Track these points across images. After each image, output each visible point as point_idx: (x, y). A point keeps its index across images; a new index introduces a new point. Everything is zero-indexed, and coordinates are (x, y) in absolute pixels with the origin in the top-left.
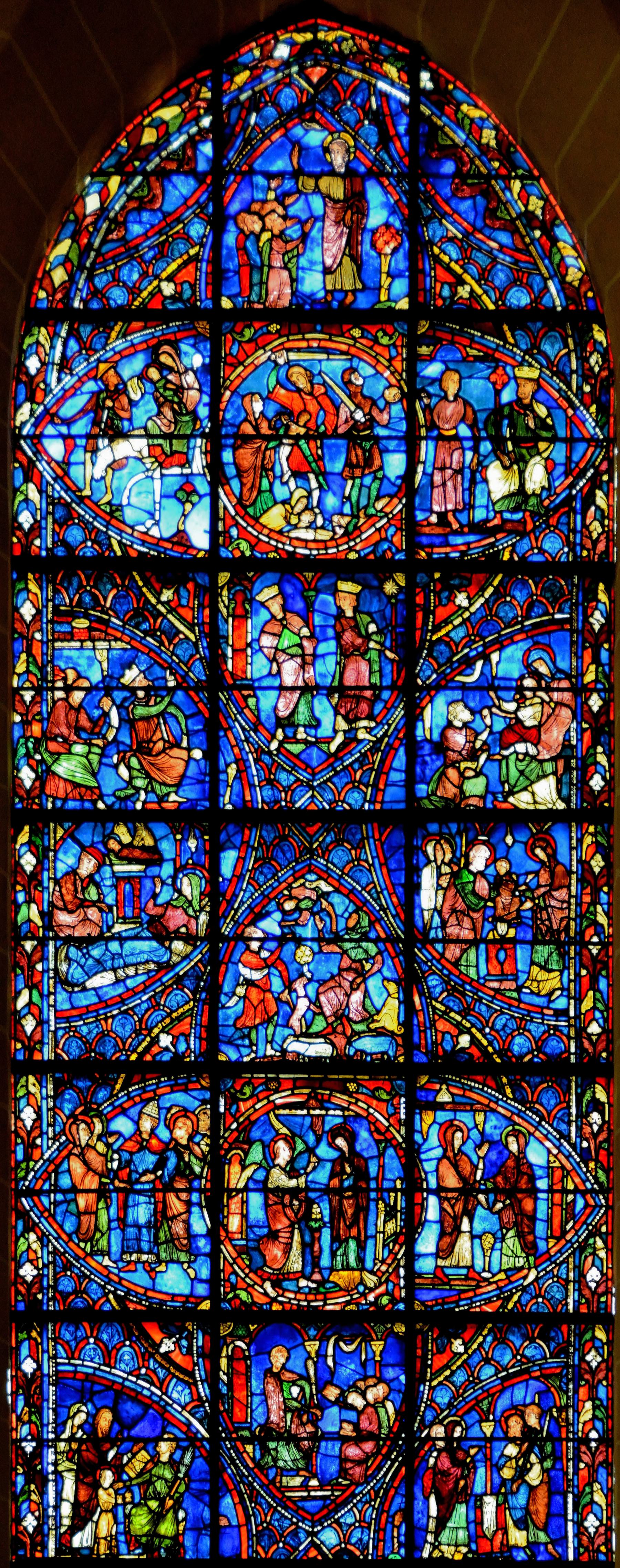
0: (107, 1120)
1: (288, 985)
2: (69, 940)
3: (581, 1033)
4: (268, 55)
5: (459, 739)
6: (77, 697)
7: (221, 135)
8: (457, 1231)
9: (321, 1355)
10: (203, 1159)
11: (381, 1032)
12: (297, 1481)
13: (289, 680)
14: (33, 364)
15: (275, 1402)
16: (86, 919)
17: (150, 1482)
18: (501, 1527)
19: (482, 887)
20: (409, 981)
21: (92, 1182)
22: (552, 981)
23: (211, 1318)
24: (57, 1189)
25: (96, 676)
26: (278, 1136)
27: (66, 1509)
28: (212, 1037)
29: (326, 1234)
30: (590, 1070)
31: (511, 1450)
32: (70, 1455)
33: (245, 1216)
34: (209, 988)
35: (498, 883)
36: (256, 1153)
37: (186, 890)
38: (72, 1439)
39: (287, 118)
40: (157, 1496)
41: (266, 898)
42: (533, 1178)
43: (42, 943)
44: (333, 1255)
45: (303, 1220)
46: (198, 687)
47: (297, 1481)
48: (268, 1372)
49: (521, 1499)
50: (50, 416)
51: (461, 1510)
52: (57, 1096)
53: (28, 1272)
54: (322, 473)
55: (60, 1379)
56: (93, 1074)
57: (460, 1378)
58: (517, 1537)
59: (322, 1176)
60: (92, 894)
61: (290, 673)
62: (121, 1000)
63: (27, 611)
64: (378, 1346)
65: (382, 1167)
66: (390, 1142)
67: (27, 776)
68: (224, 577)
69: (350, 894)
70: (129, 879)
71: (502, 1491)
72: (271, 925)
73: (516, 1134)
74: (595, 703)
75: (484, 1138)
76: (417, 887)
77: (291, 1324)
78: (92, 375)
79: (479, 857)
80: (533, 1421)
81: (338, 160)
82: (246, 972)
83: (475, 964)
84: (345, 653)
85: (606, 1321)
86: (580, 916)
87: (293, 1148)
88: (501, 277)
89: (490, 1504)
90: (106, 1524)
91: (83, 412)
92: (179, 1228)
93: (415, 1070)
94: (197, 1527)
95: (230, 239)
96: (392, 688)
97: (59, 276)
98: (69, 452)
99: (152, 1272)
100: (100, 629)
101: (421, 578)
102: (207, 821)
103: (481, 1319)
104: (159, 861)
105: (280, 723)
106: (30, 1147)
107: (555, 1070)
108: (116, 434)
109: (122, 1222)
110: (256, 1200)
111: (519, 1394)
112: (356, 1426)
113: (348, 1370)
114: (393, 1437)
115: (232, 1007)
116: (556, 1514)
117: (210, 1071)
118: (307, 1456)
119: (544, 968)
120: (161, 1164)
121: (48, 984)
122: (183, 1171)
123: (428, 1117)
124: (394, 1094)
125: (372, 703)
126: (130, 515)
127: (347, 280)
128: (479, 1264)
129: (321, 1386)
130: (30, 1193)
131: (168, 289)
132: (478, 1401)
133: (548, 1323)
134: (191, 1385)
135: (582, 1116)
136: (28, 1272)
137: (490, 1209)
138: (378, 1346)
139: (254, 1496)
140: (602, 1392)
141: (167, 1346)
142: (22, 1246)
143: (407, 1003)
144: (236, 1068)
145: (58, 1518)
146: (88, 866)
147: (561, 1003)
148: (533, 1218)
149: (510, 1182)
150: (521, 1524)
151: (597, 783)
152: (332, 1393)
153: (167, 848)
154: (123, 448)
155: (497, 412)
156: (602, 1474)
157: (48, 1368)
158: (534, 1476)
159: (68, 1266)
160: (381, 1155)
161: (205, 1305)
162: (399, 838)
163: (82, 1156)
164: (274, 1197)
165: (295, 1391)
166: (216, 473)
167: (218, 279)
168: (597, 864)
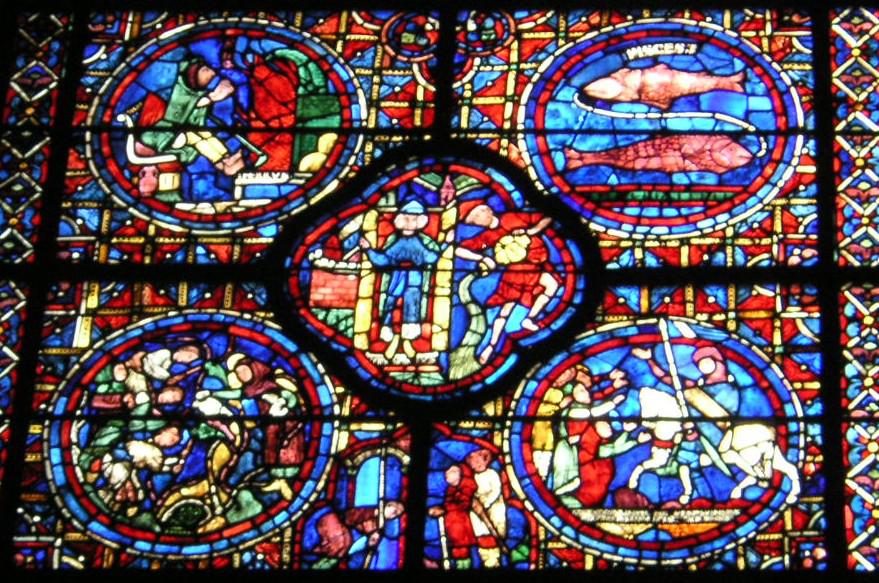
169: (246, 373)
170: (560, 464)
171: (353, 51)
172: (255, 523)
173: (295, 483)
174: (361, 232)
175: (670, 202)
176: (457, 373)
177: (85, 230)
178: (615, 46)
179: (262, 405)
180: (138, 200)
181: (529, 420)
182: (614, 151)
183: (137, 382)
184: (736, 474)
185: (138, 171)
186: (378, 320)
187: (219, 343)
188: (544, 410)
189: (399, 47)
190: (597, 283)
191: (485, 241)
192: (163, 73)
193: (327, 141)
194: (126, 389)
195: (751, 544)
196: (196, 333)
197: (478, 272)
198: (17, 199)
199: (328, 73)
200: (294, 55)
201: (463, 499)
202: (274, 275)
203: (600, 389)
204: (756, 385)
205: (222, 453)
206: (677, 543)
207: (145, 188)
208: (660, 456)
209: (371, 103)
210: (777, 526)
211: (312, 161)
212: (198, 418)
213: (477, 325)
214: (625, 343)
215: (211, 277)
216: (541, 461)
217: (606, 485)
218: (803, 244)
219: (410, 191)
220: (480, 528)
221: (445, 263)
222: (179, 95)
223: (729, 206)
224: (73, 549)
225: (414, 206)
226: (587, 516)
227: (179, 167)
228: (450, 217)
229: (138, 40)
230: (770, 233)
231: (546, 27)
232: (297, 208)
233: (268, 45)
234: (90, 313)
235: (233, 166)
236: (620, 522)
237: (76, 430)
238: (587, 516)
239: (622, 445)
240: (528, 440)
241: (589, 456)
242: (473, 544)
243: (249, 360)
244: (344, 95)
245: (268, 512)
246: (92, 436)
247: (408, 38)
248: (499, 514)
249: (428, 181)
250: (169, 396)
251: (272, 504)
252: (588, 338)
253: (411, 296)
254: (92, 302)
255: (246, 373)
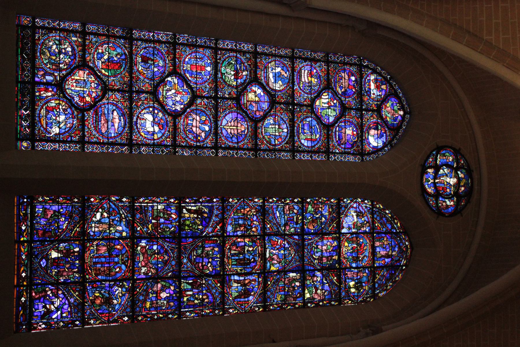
0: (256, 215)
1: (278, 249)
2: (284, 208)
3: (270, 305)
4: (407, 241)
5: (315, 279)
6: (320, 209)
7: (396, 233)
8: (238, 283)
9: (217, 258)
10: (250, 233)
11: (270, 267)
12: (195, 254)
13: (323, 247)
14: (366, 201)
15: (209, 249)
16: (287, 211)
17: (195, 224)
18: (187, 295)
19: (293, 285)
20: (278, 272)
21: (246, 212)
22: (279, 299)
23: (223, 236)
24: (244, 205)
25: (323, 213)
26: (253, 248)
27: (190, 208)
28: (269, 235)
29: (237, 258)
30: (265, 307)
31: (201, 297)
32: (199, 208)
33: (240, 242)
34: (277, 234)
35: (294, 287)
36: (251, 244)
37: (292, 230)
38: (202, 209)
39: (398, 244)
40: (192, 226)
41: (291, 244)
42: (247, 298)
43: (283, 203)
44: (234, 259)
45: (240, 253)
46: (322, 231)
47: (195, 254)
48: (214, 247)
49: (192, 299)
50: (359, 204)
51: (190, 287)
52: (260, 206)
53: (231, 200)
54: (352, 252)
55: (213, 206)
56: (263, 212)
57: (213, 285)
58: (185, 299)
59: (247, 257)
60: (291, 212)
61: (324, 248)
62: (275, 218)
63: (332, 200)
64: (218, 269)
65: (248, 268)
66: (253, 270)
67: (309, 200)
68: (338, 235)
69: (292, 260)
70: (293, 219)
71: (193, 295)
72: (287, 246)
73: (254, 294)
74: (321, 303)
75: (253, 288)
76: (293, 273)
77: (222, 252)
78: (365, 212)
79: (298, 284)
80: (206, 300)
81: (394, 253)
82: (279, 241)
83: (281, 284)
84: (327, 258)
85: (223, 314)
86: (289, 303)
87: (252, 251)
88: (379, 282)
89: (191, 293)
90: (187, 215)
91: (360, 210)
92: (238, 229)
93: (265, 273)
94: (187, 234)
95: (383, 235)
96: (323, 267)
97: (378, 206)
98: (355, 208)
99: (231, 224)
100: (330, 213)
101: (338, 271)
102: (303, 233)
103: (223, 289)
104: (296, 225)
105: (317, 246)
106: (251, 200)
107: (265, 301)
108: (357, 216)
109: (239, 218)
110: (243, 244)
111: (211, 297)
112: (205, 265)
113: (214, 263)
114: (203, 272)
115: (274, 239)
116: (188, 306)
117: (264, 235)
118: (199, 256)
119: (281, 297)
120: (249, 225)
121: (277, 204)
122: (248, 230)
123: (257, 277)
124: (260, 270)
125: (320, 263)
126: (346, 218)
127: (378, 256)
128: (233, 288)
129: (211, 258)
130: (244, 200)
131: (376, 225)
132: (209, 289)
133: (223, 302)
134: (212, 232)
135: (257, 306)
136: (231, 200)
137: (242, 290)
138: (218, 269)
139: (192, 245)
140: (211, 314)
141: (218, 227)
142: (235, 199)
143: (275, 271)
144: (264, 240)
145: (188, 206)
146: (295, 211)
147: (275, 301)
148: (240, 298)
149: (246, 293)
150: (187, 299)
151: (309, 305)
152: (210, 260)
153: (298, 226)
154: (355, 217)
155: (361, 283)
156: (197, 315)
157: (214, 204)
158: (196, 301)
159: (232, 208)
160: (250, 268)
161: (225, 235)
162: (300, 269)
163: (250, 210)
164: (243, 248)
165: (211, 253)
166: (352, 234)
167: (378, 233)
168: (297, 306)
169: (67, 61)
170: (53, 104)
171: (123, 78)
172: (43, 62)
173: (49, 68)
174: (91, 78)
175: (95, 122)
176: (67, 90)
177: (92, 39)
178: (123, 115)
179: (62, 64)
180: (97, 47)
181: (59, 100)
182: (104, 114)
183: (66, 46)
184: (51, 128)
185: (102, 47)
186: (76, 80)
187: (72, 58)
188: (61, 102)
189: (123, 84)
190: (82, 110)
191: (89, 95)
192: (119, 50)
193: (107, 74)
194: (64, 45)
195: (40, 129)
196: (74, 54)
197: (84, 94)
198: (97, 29)
199: (119, 74)
200: (122, 69)
201: (47, 90)
202: (83, 65)
203: (64, 110)
204: (65, 131)
205: (54, 58)
206: (40, 119)
207: (99, 48)
208: (54, 118)
209: (113, 80)
210: (42, 133)
211: (103, 71)
212: (60, 55)
213: (75, 94)
214: (73, 114)
215: (83, 57)
216: (53, 101)
217: (49, 110)
218: (89, 139)
219: (98, 85)
220: (42, 93)
221: (85, 89)
222: (115, 53)
223: (95, 130)
224: (39, 37)
225: (96, 85)
226: (44, 107)
227: (103, 53)
228: (94, 90)
229: (125, 47)
230: (91, 135)
231: (127, 105)
232: (95, 69)
233: (124, 66)
234: (78, 40)
235: (103, 60)
236: (43, 112)
237: (58, 38)
238: (44, 107)
239: (56, 113)
240: (56, 100)
241: (53, 108)
242: (40, 91)
243: (69, 62)
244: (115, 76)
245: (44, 64)
246: (57, 40)
247: (125, 86)
248: (45, 95)
249: (100, 87)
250: (63, 51)
251: (46, 65)
252: (73, 109)
253: (80, 85)
254: (80, 40)
255: (67, 61)
